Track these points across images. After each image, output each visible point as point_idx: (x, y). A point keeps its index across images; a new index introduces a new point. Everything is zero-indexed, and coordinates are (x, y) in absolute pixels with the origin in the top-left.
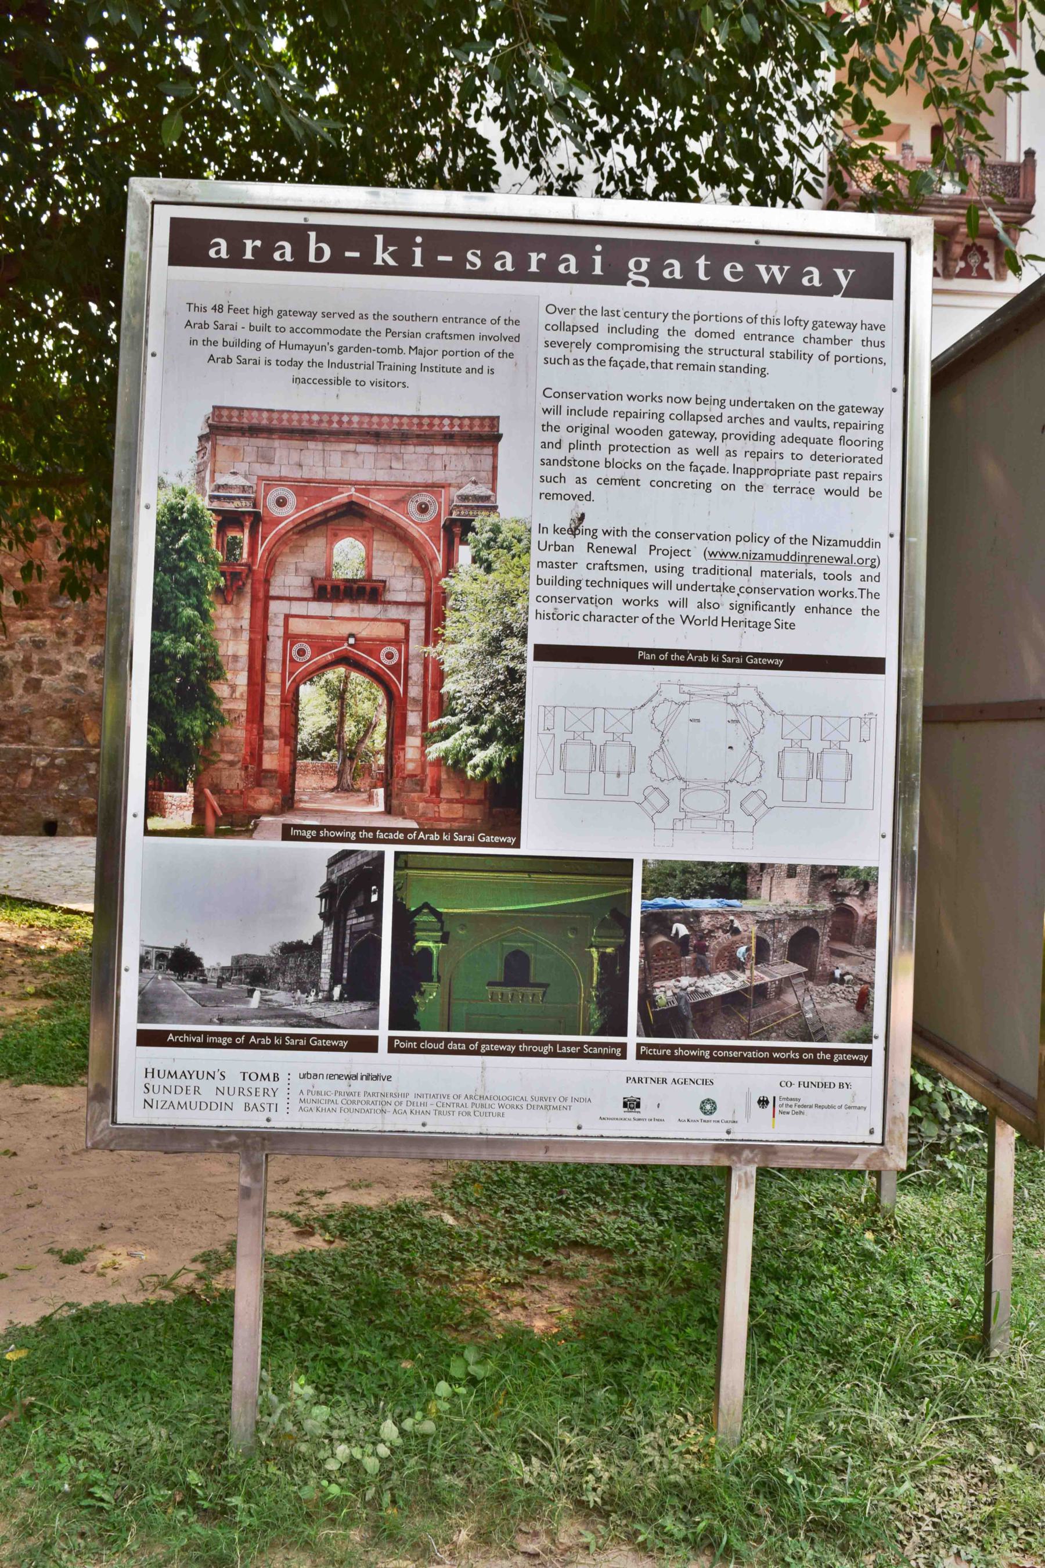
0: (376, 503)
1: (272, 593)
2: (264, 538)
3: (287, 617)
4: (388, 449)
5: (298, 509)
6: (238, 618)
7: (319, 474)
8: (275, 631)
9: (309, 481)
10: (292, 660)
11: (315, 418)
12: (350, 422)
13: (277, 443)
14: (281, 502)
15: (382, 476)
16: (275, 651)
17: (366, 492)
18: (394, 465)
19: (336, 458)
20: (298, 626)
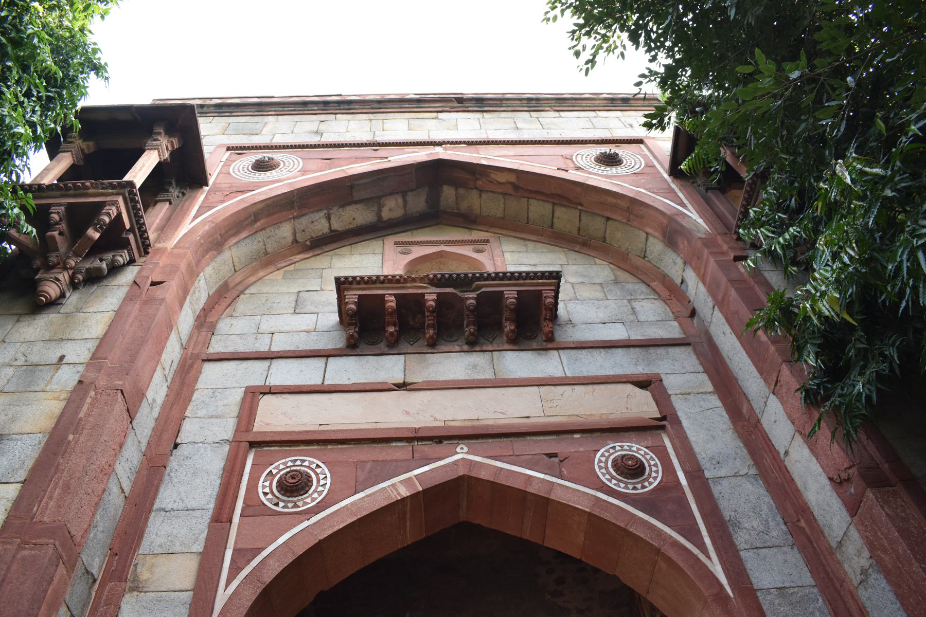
1: (217, 346)
5: (304, 171)
10: (254, 508)
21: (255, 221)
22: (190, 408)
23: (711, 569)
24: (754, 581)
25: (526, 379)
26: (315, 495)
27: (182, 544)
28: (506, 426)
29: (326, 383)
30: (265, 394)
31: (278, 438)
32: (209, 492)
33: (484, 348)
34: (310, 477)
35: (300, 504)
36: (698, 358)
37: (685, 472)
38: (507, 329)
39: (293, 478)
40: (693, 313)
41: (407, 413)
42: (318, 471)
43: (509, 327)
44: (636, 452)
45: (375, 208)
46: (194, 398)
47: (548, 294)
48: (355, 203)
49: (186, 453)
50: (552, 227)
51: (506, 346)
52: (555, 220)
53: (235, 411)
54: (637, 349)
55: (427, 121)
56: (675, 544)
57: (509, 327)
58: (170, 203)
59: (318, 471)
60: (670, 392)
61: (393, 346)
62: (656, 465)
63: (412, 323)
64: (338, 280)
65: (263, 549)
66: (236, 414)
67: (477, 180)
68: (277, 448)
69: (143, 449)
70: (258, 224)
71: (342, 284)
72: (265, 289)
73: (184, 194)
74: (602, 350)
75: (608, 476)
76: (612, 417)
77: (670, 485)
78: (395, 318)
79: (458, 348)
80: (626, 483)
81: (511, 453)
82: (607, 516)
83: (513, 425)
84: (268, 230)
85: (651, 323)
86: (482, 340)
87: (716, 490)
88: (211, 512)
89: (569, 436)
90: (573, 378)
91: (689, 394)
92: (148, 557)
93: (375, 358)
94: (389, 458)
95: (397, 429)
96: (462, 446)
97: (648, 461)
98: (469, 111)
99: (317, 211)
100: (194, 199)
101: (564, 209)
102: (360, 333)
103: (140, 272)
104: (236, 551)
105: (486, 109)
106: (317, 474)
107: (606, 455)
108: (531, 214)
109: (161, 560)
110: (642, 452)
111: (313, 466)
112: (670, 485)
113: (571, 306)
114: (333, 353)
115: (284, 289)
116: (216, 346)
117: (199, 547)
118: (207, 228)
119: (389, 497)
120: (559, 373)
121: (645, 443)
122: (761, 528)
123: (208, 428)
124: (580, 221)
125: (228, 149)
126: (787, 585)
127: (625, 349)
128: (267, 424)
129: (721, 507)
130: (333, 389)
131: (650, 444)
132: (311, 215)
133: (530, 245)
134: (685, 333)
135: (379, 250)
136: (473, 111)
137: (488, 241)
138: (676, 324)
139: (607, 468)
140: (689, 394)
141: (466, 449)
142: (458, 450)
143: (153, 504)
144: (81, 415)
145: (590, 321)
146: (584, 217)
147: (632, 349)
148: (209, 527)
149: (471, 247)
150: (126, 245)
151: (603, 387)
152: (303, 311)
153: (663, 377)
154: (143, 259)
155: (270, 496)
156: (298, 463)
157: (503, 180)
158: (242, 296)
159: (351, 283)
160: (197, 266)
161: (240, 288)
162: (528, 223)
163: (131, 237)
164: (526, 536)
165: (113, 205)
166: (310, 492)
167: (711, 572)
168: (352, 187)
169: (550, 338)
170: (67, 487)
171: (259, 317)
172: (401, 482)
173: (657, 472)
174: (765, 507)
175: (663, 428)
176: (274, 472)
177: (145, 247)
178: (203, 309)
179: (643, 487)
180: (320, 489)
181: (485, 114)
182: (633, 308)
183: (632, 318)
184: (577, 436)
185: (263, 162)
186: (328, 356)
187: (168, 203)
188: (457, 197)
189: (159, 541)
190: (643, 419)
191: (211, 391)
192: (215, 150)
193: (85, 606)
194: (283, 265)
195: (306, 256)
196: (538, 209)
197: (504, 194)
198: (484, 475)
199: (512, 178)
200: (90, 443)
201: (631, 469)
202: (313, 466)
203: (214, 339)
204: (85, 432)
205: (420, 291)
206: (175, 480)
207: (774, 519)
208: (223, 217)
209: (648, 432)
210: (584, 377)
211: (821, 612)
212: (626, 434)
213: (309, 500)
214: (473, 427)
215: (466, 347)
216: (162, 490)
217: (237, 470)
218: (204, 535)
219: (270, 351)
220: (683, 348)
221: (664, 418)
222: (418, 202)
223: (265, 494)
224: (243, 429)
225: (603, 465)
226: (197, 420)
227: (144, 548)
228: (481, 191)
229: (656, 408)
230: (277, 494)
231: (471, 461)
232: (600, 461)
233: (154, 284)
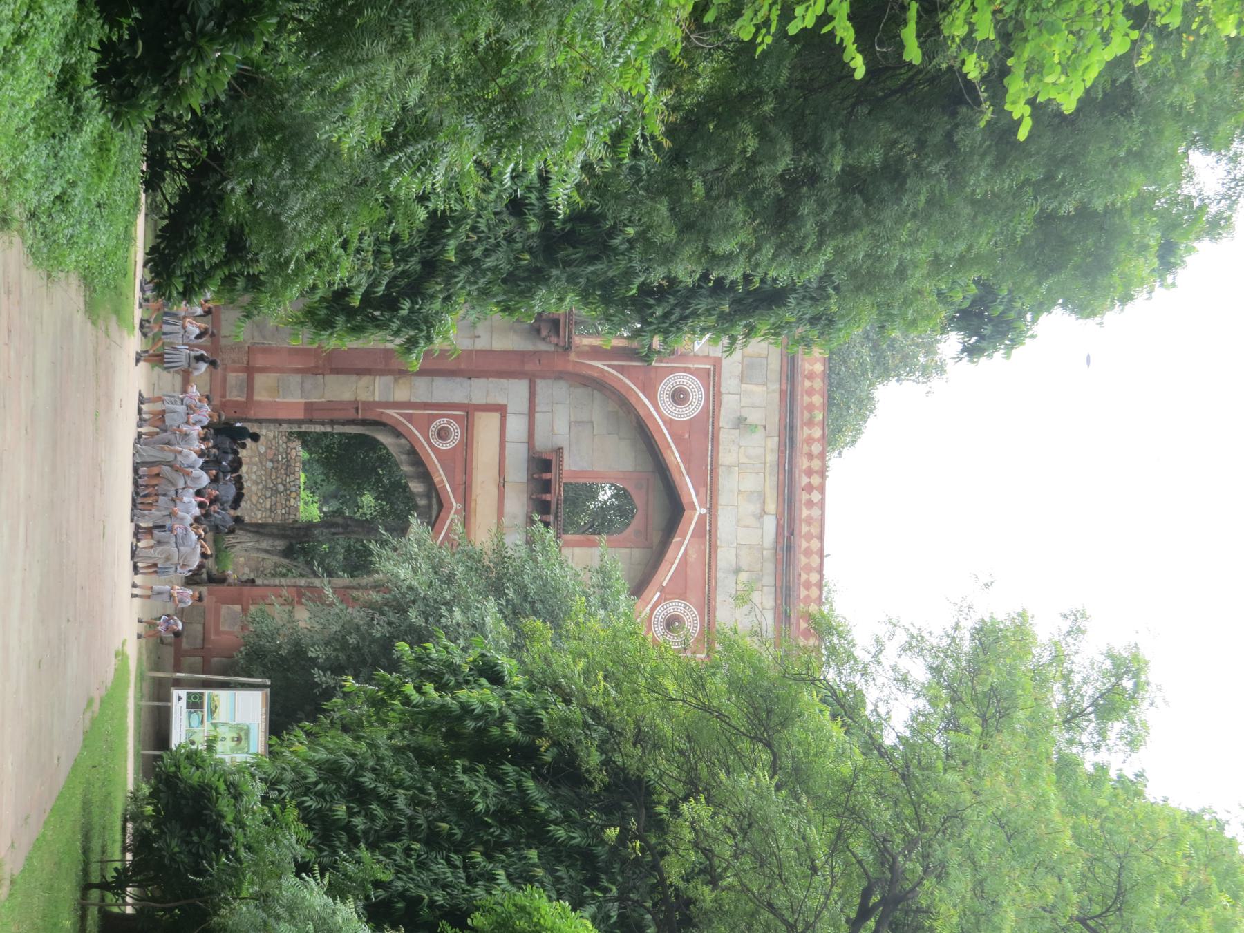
0: (683, 547)
1: (541, 385)
2: (621, 369)
3: (502, 410)
4: (769, 567)
5: (669, 423)
6: (492, 331)
7: (727, 456)
9: (715, 440)
12: (810, 504)
13: (776, 386)
14: (679, 396)
15: (725, 557)
17: (700, 532)
18: (743, 577)
19: (751, 483)
20: (486, 426)
53: (491, 401)
71: (559, 451)
103: (547, 352)
136: (777, 541)
203: (549, 382)
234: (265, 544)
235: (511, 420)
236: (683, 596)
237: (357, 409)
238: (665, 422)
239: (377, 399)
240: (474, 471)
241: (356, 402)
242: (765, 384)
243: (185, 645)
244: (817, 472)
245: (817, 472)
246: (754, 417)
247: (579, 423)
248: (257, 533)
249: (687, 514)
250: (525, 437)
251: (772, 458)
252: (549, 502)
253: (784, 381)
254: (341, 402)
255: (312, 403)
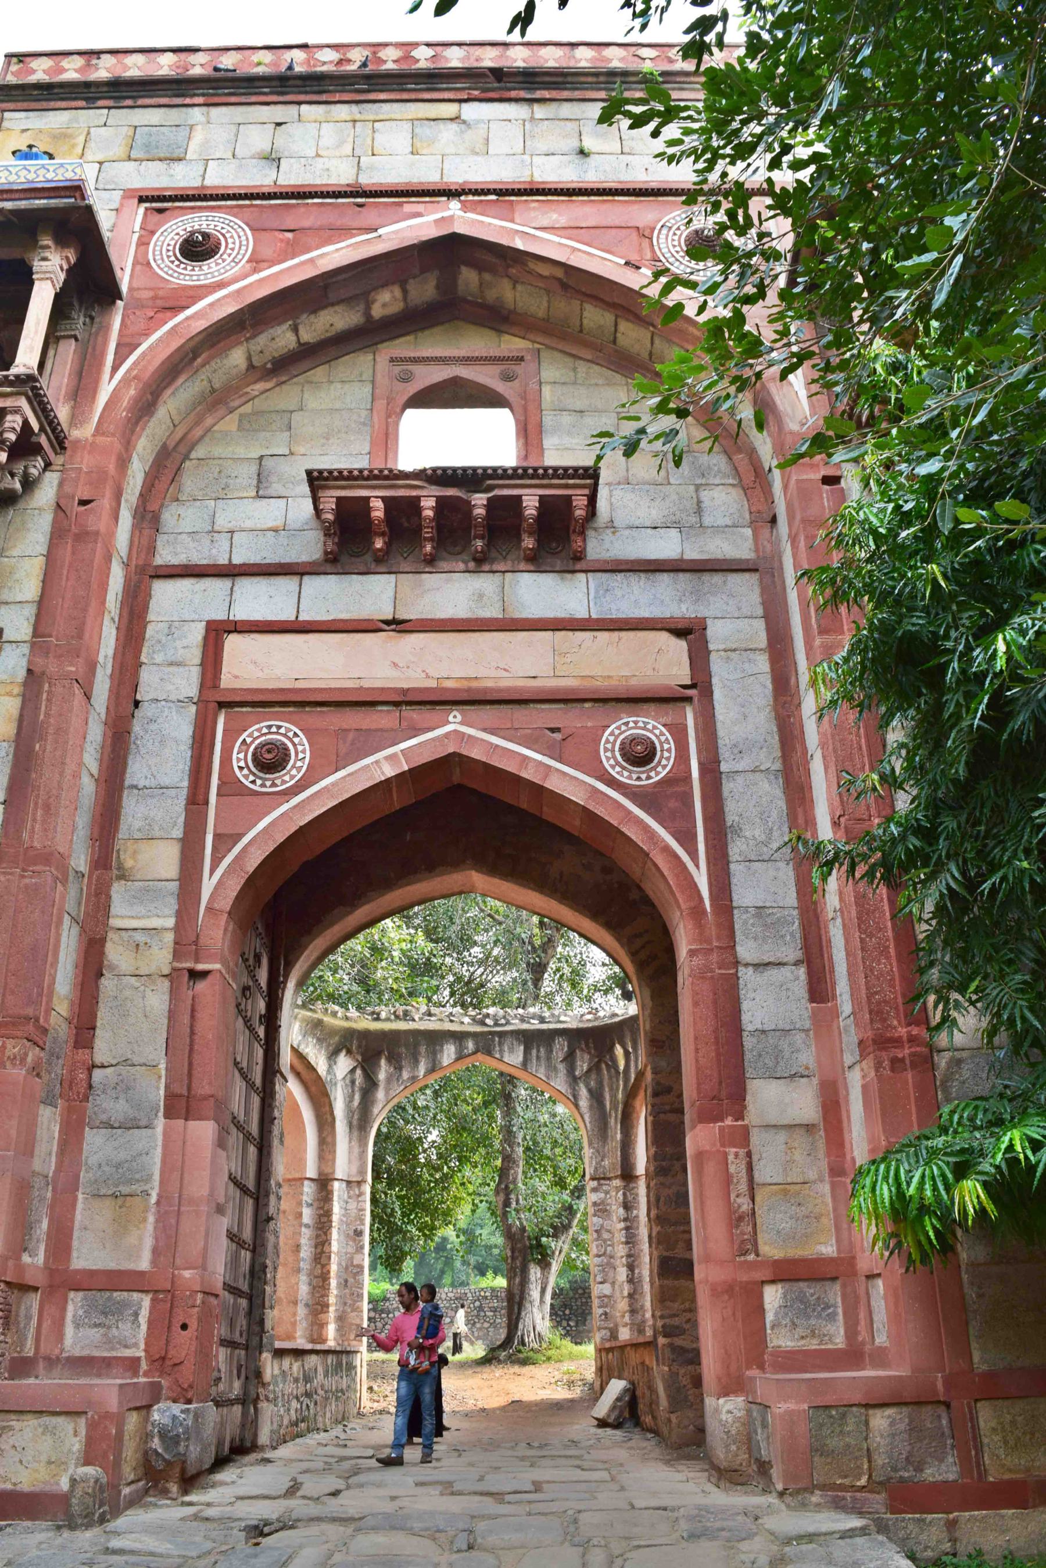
1: (166, 555)
3: (217, 633)
5: (257, 262)
7: (339, 173)
8: (170, 681)
10: (230, 787)
11: (329, 56)
13: (197, 114)
14: (198, 249)
16: (162, 757)
18: (588, 144)
21: (194, 358)
22: (145, 650)
23: (696, 880)
24: (735, 897)
25: (540, 620)
26: (294, 772)
27: (161, 828)
28: (508, 689)
29: (301, 618)
30: (229, 632)
31: (249, 698)
32: (181, 767)
33: (495, 567)
34: (287, 749)
35: (278, 782)
36: (762, 594)
37: (700, 763)
38: (524, 544)
39: (269, 751)
40: (774, 520)
41: (395, 665)
42: (296, 740)
43: (529, 542)
44: (651, 732)
45: (362, 307)
46: (147, 636)
47: (580, 502)
48: (333, 305)
49: (149, 714)
50: (614, 342)
51: (522, 566)
52: (619, 335)
53: (195, 656)
54: (688, 575)
55: (441, 125)
56: (667, 849)
57: (529, 542)
58: (76, 340)
59: (296, 740)
60: (711, 647)
61: (382, 563)
62: (669, 750)
63: (406, 524)
64: (309, 473)
65: (244, 835)
66: (198, 661)
67: (508, 266)
68: (249, 709)
69: (103, 716)
70: (199, 360)
71: (317, 480)
72: (218, 451)
73: (92, 318)
74: (642, 575)
75: (612, 762)
76: (633, 682)
77: (679, 779)
78: (384, 528)
79: (461, 566)
80: (630, 772)
81: (509, 726)
82: (600, 811)
83: (515, 689)
84: (213, 364)
85: (718, 529)
86: (494, 554)
87: (728, 787)
88: (184, 793)
89: (579, 705)
90: (598, 620)
91: (735, 650)
92: (129, 843)
93: (360, 577)
94: (374, 726)
95: (383, 689)
96: (455, 713)
97: (661, 744)
98: (509, 100)
99: (279, 324)
100: (107, 329)
101: (630, 325)
102: (342, 544)
103: (61, 484)
104: (217, 836)
105: (538, 94)
106: (294, 745)
107: (622, 728)
108: (585, 322)
109: (143, 846)
110: (657, 732)
111: (291, 734)
112: (679, 779)
113: (618, 493)
114: (308, 570)
115: (241, 452)
116: (164, 553)
117: (178, 832)
118: (132, 392)
119: (372, 777)
120: (582, 613)
121: (663, 720)
122: (763, 837)
123: (170, 681)
124: (652, 343)
125: (142, 200)
126: (768, 904)
127: (672, 574)
128: (236, 677)
129: (727, 810)
130: (309, 627)
131: (668, 720)
132: (271, 331)
133: (582, 367)
134: (757, 550)
135: (367, 375)
136: (517, 100)
137: (522, 359)
138: (748, 532)
139: (613, 751)
140: (735, 650)
141: (459, 718)
142: (451, 718)
143: (123, 781)
144: (42, 717)
145: (637, 523)
146: (657, 341)
147: (681, 575)
148: (186, 810)
149: (496, 370)
150: (38, 449)
151: (631, 634)
152: (271, 492)
153: (709, 622)
154: (58, 460)
155: (245, 771)
156: (274, 729)
157: (546, 273)
158: (188, 463)
159: (327, 479)
160: (127, 450)
161: (182, 449)
162: (581, 331)
163: (43, 440)
164: (525, 806)
165: (16, 412)
166: (289, 767)
167: (695, 885)
168: (326, 287)
169: (579, 556)
170: (47, 807)
171: (212, 502)
172: (386, 758)
173: (668, 759)
174: (774, 814)
175: (688, 699)
176: (249, 740)
177: (60, 443)
178: (141, 495)
179: (649, 778)
180: (299, 764)
181: (536, 107)
182: (699, 502)
183: (694, 519)
184: (587, 705)
185: (197, 244)
186: (302, 574)
187: (73, 341)
188: (481, 284)
189: (138, 824)
190: (669, 688)
191: (164, 625)
192: (122, 205)
193: (80, 904)
194: (236, 403)
195: (269, 385)
196: (595, 317)
197: (548, 292)
198: (476, 754)
199: (559, 273)
200: (58, 753)
201: (639, 755)
202: (291, 734)
203: (161, 540)
204: (50, 738)
205: (414, 493)
206: (143, 751)
207: (780, 828)
208: (151, 369)
209: (671, 705)
210: (611, 620)
211: (792, 934)
212: (646, 706)
213: (287, 778)
214: (469, 690)
215: (472, 565)
216: (130, 762)
217: (208, 740)
218: (182, 819)
219: (230, 564)
220: (747, 575)
221: (693, 686)
222: (424, 290)
223: (241, 768)
224: (209, 684)
225: (609, 746)
226: (155, 668)
227: (122, 833)
228: (515, 282)
229: (687, 670)
230: (253, 769)
231: (464, 734)
232: (607, 741)
233: (83, 503)
234: (535, 1293)
235: (241, 613)
236: (645, 234)
237: (196, 975)
238: (255, 271)
239: (171, 922)
240: (366, 684)
241: (172, 976)
242: (191, 127)
243: (944, 1470)
244: (375, 53)
245: (375, 53)
246: (257, 139)
247: (261, 478)
248: (520, 1305)
249: (460, 229)
250: (288, 584)
251: (343, 111)
252: (439, 499)
253: (188, 101)
254: (172, 1015)
255: (171, 1097)
